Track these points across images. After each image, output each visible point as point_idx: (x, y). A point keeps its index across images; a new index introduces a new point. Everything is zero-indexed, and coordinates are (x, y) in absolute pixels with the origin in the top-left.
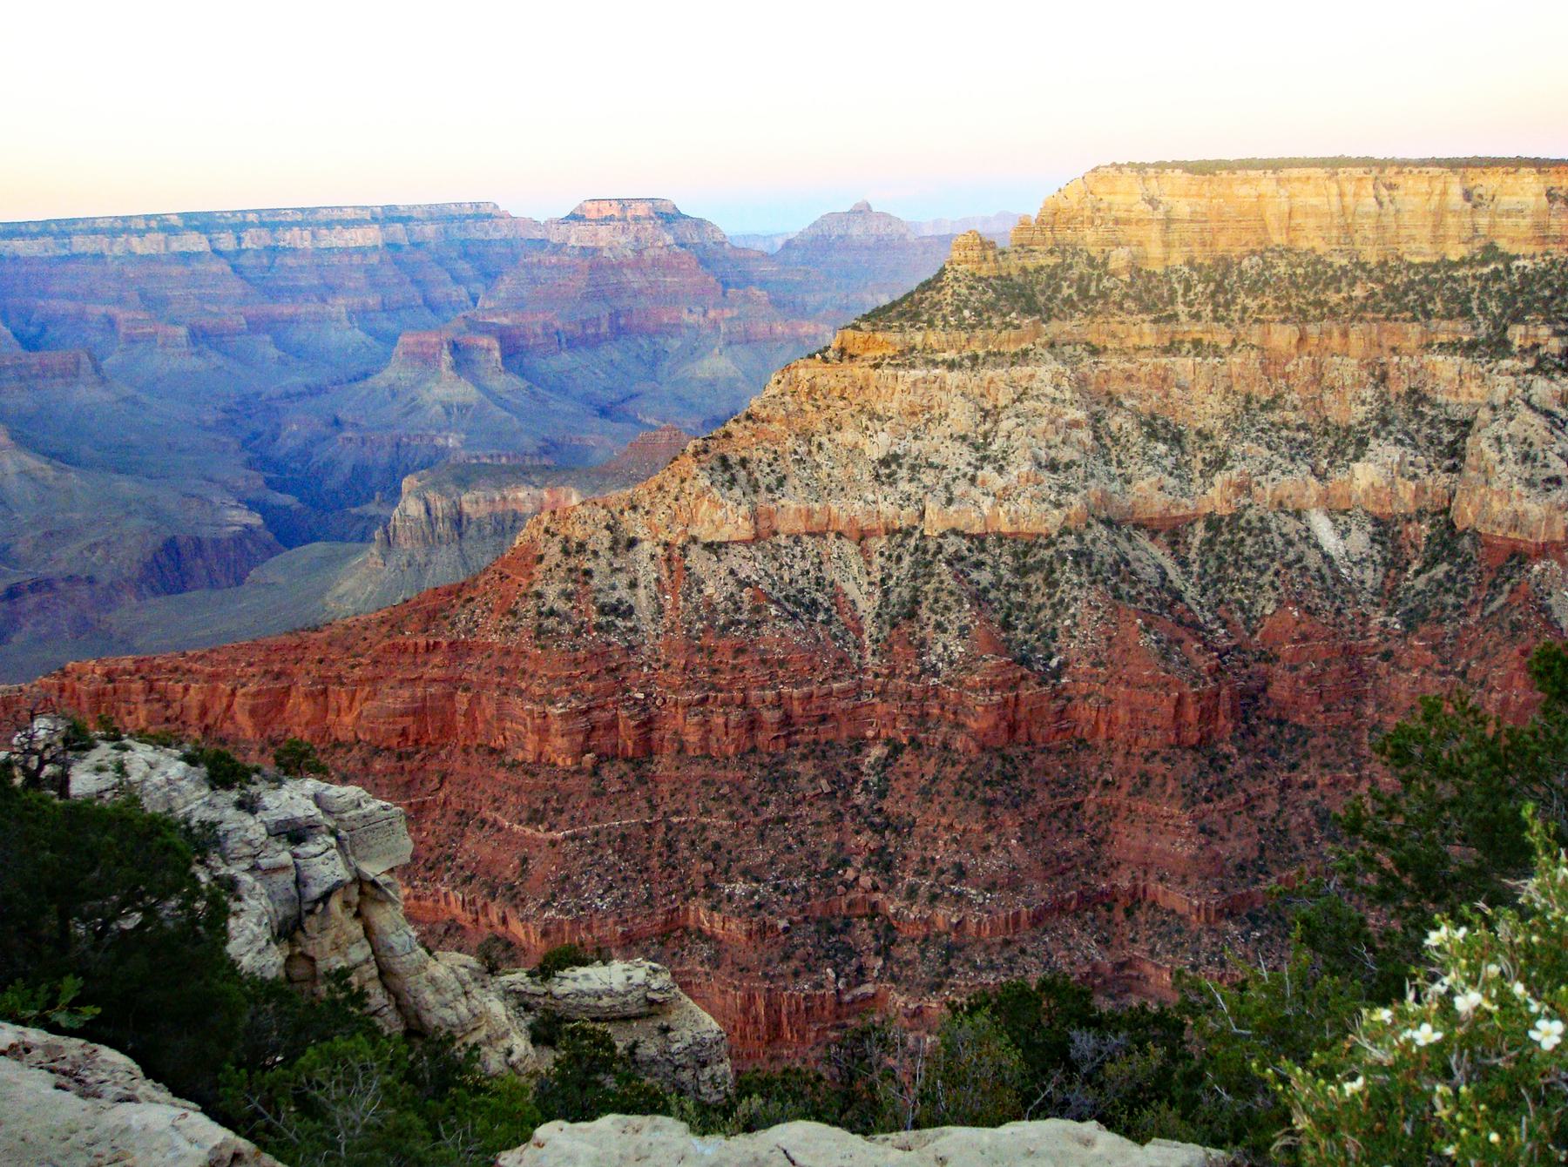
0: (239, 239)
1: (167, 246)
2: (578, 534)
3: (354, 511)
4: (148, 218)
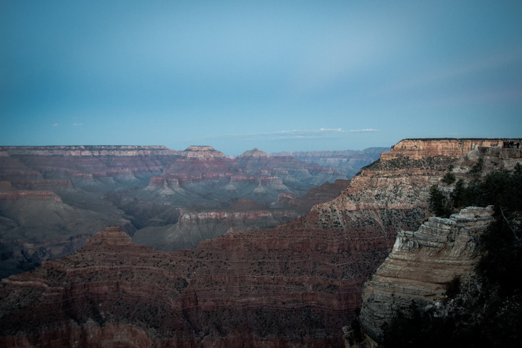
0: (100, 153)
1: (81, 154)
2: (324, 208)
3: (150, 220)
4: (76, 146)
